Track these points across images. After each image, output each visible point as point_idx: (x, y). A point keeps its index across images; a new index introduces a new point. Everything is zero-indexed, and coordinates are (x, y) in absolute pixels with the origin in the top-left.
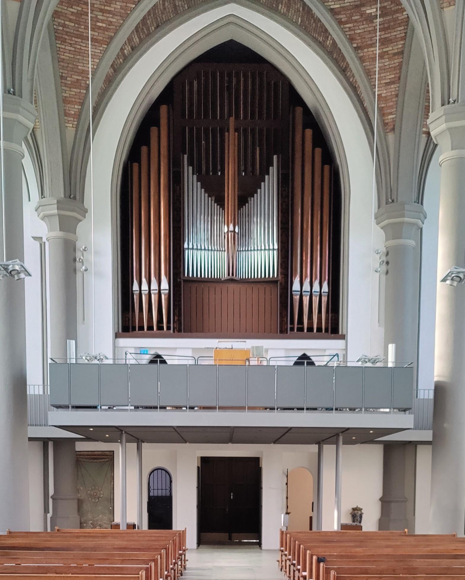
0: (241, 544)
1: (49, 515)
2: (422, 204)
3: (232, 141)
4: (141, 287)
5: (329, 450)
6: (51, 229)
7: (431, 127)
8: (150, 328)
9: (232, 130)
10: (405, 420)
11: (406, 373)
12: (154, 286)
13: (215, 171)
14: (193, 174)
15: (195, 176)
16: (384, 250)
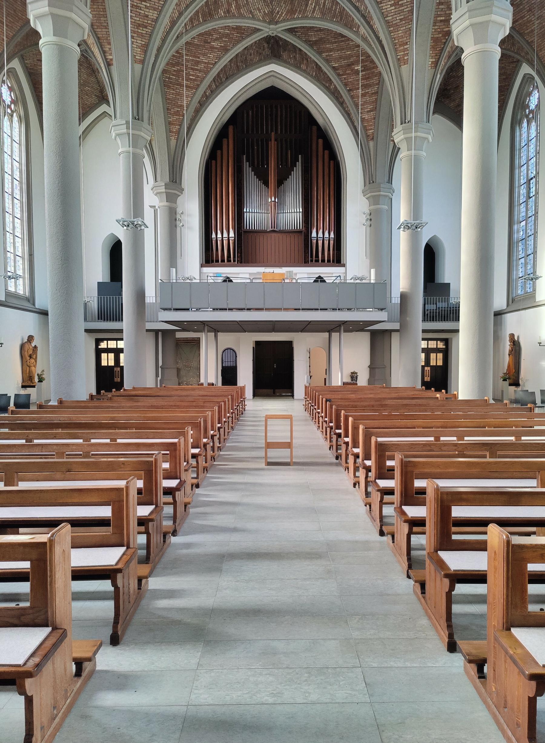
0: (281, 396)
1: (159, 379)
2: (391, 184)
3: (273, 145)
4: (217, 236)
5: (335, 335)
6: (161, 201)
7: (395, 137)
8: (223, 261)
9: (273, 139)
10: (382, 316)
11: (382, 286)
12: (225, 235)
13: (263, 166)
14: (249, 167)
15: (250, 168)
16: (369, 212)
